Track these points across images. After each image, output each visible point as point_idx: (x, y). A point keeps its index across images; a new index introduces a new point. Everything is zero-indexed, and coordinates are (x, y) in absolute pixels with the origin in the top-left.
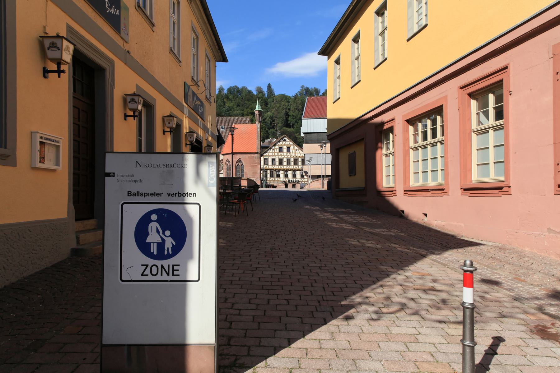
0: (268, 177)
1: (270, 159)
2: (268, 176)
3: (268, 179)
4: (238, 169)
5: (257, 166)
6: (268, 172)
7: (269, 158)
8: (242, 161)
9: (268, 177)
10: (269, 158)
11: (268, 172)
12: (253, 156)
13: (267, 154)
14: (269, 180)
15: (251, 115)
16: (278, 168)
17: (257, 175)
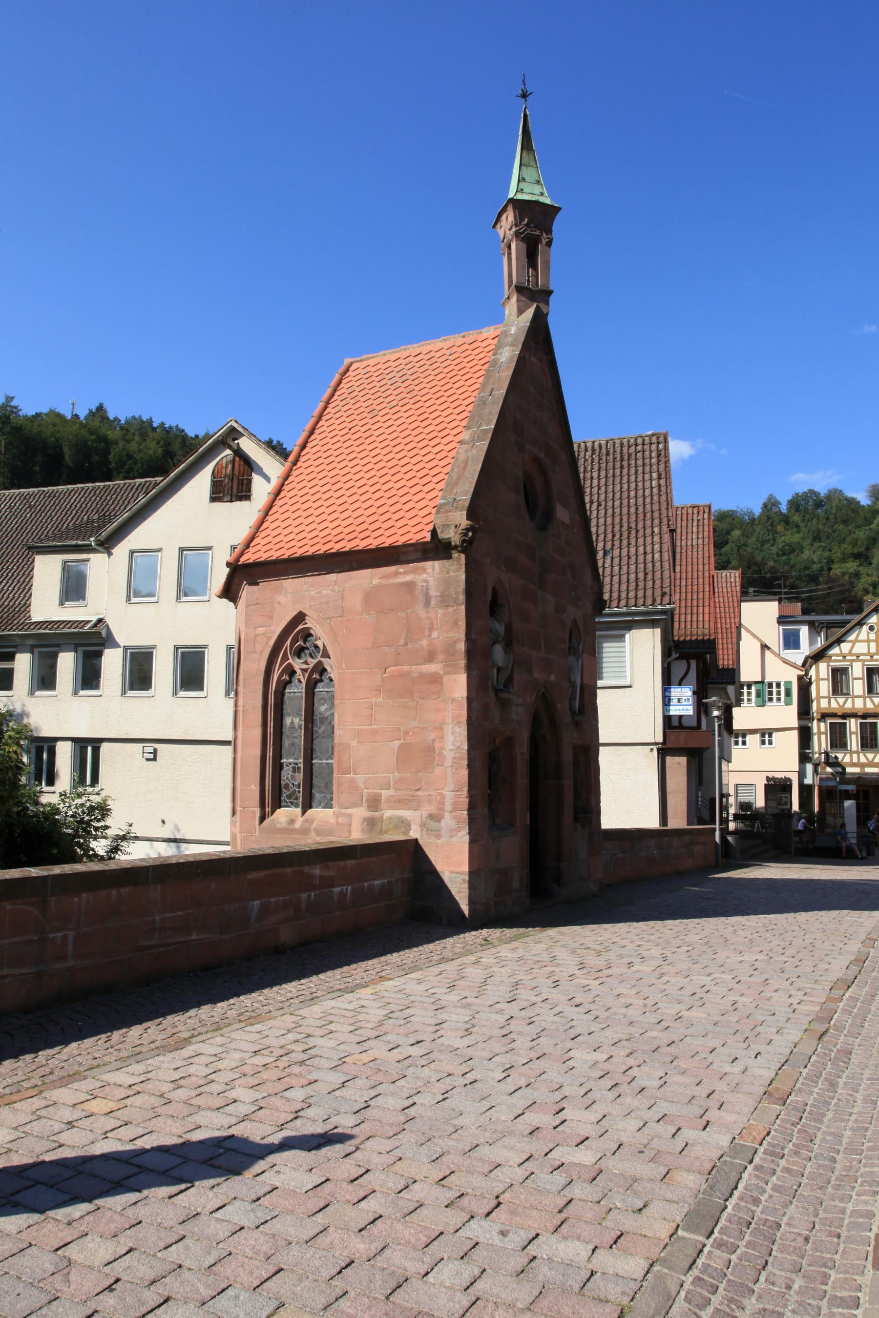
0: (854, 748)
1: (857, 671)
2: (854, 741)
3: (855, 756)
4: (288, 721)
5: (435, 679)
6: (853, 725)
7: (854, 664)
8: (319, 643)
9: (854, 748)
10: (854, 664)
11: (853, 725)
12: (410, 586)
13: (845, 647)
14: (855, 760)
15: (853, 562)
16: (862, 706)
17: (438, 771)
